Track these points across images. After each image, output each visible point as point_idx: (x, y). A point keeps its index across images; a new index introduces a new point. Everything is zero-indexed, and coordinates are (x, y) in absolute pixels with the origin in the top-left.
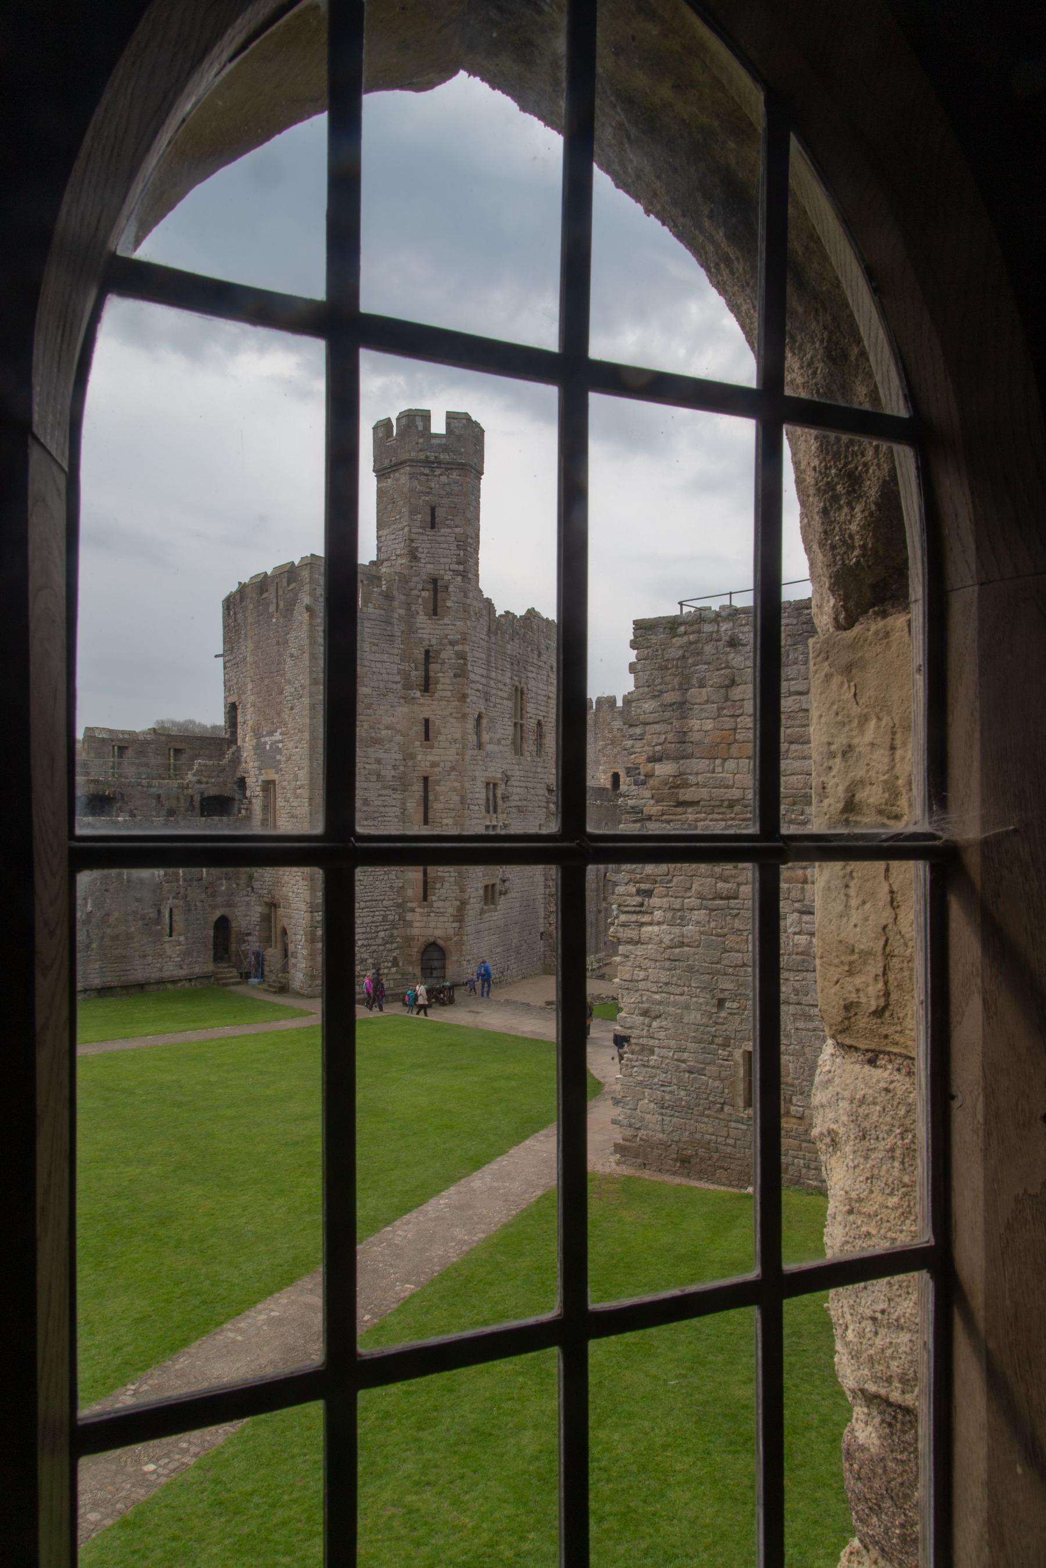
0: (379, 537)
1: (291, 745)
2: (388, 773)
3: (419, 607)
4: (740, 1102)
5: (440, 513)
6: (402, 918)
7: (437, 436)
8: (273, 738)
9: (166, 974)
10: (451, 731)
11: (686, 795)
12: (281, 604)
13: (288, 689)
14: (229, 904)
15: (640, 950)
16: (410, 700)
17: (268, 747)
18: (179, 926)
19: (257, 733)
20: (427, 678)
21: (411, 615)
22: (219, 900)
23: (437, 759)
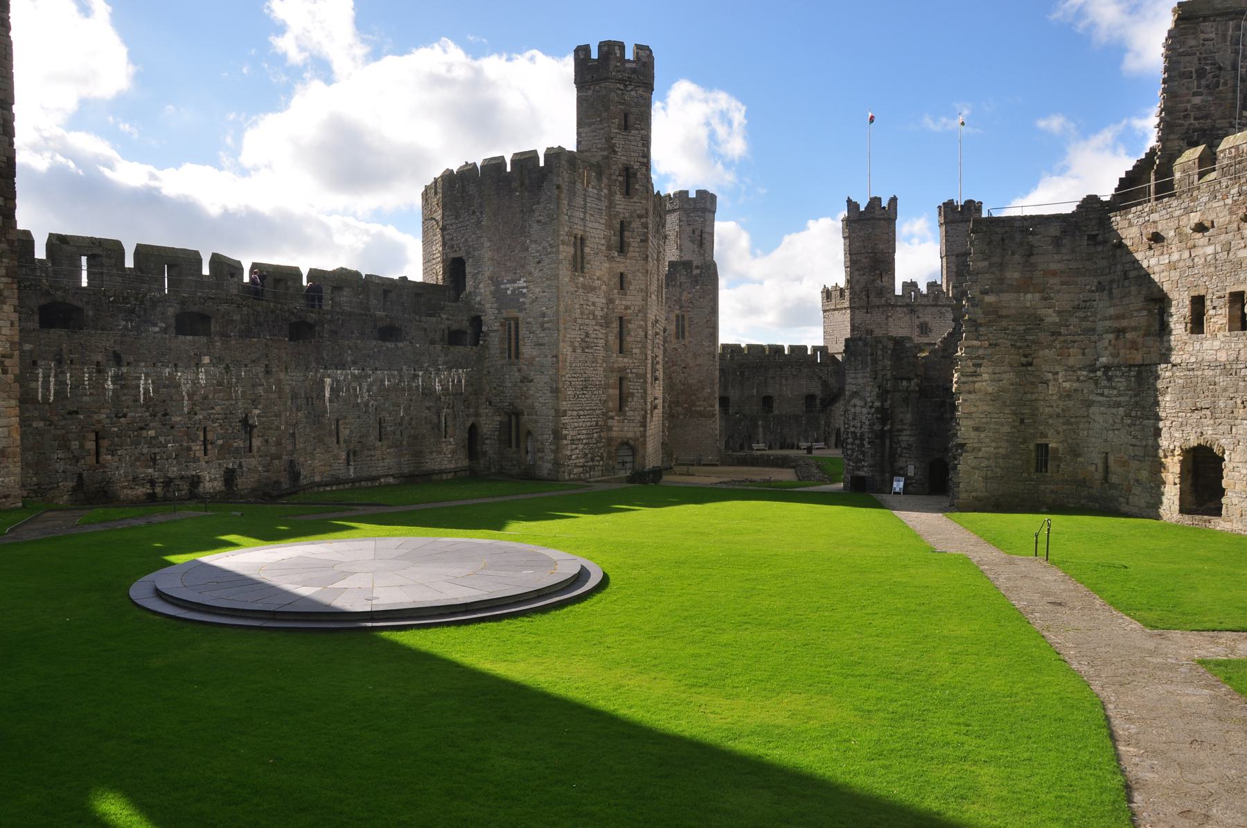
0: (578, 134)
1: (537, 290)
2: (598, 313)
4: (1032, 470)
6: (606, 423)
7: (629, 61)
9: (443, 467)
10: (636, 284)
11: (1004, 312)
12: (527, 182)
14: (477, 415)
15: (972, 396)
16: (611, 259)
18: (450, 430)
19: (495, 281)
21: (611, 194)
22: (471, 410)
23: (629, 303)
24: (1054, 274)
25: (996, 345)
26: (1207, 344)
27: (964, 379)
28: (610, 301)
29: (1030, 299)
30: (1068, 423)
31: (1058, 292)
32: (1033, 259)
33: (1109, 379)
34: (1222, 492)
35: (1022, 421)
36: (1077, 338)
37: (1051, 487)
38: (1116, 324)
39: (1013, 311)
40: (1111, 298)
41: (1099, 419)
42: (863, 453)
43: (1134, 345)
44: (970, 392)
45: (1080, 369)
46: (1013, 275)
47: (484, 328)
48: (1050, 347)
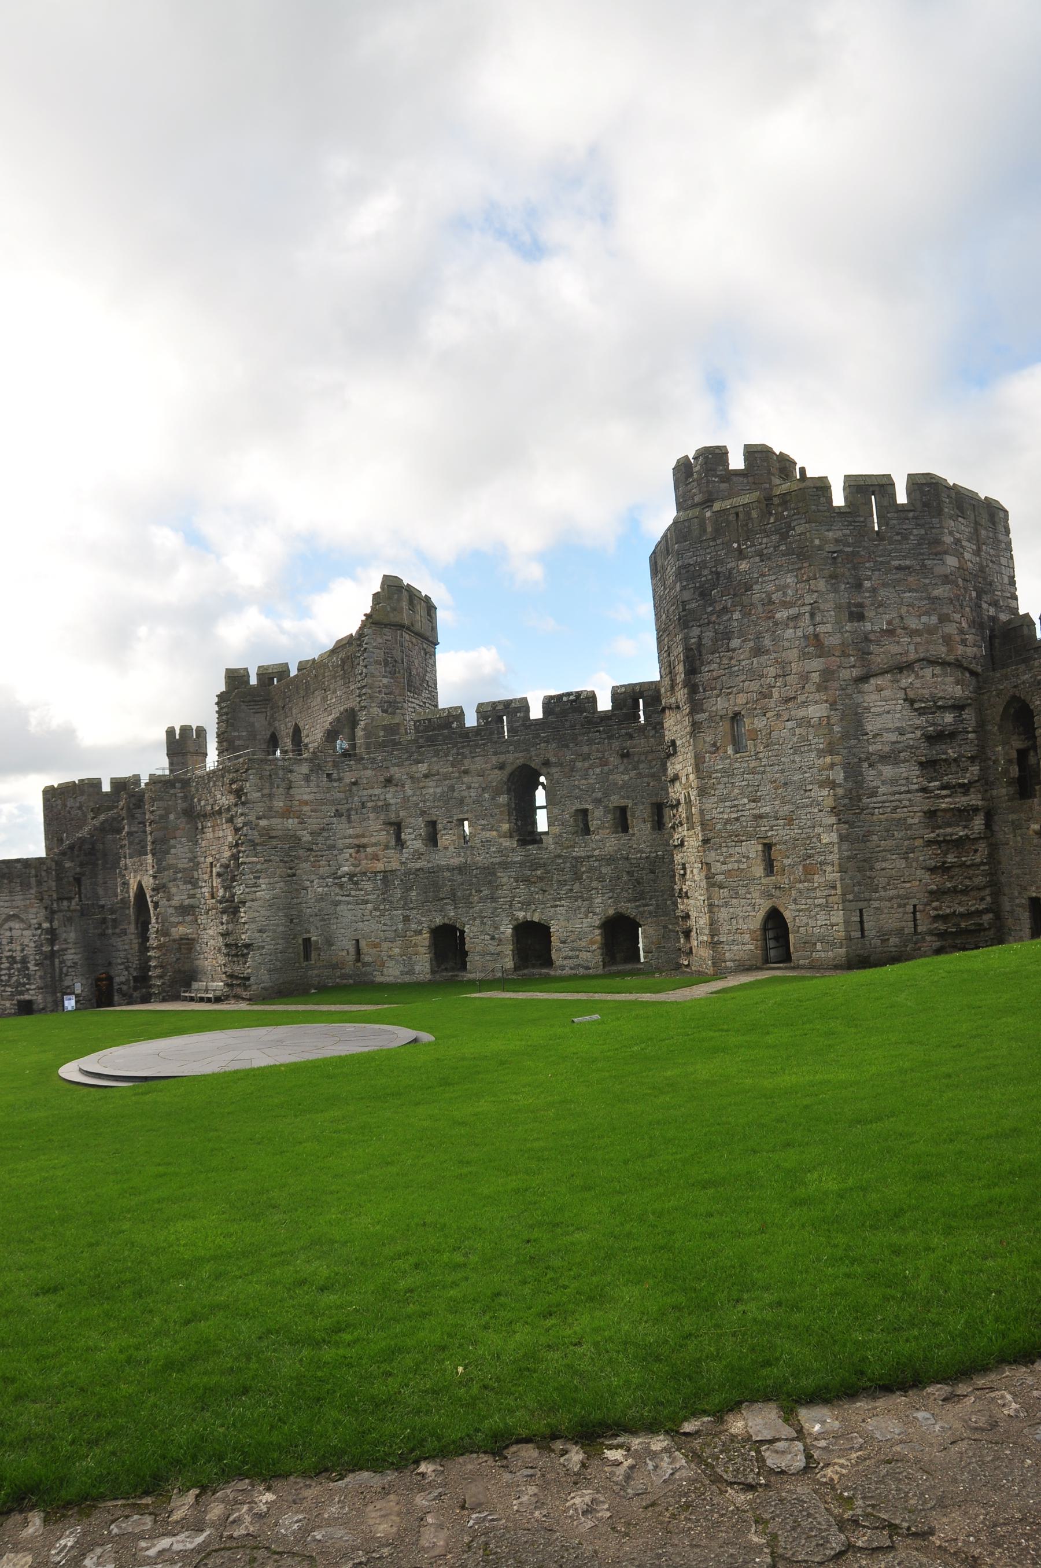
11: (273, 833)
15: (255, 904)
24: (306, 803)
25: (270, 861)
26: (441, 854)
27: (247, 890)
29: (291, 823)
30: (323, 920)
31: (310, 817)
32: (292, 791)
33: (356, 883)
34: (465, 954)
35: (291, 921)
36: (324, 853)
37: (316, 972)
38: (356, 841)
39: (280, 833)
40: (349, 822)
41: (349, 914)
42: (28, 977)
43: (376, 857)
44: (253, 900)
45: (328, 877)
48: (306, 861)
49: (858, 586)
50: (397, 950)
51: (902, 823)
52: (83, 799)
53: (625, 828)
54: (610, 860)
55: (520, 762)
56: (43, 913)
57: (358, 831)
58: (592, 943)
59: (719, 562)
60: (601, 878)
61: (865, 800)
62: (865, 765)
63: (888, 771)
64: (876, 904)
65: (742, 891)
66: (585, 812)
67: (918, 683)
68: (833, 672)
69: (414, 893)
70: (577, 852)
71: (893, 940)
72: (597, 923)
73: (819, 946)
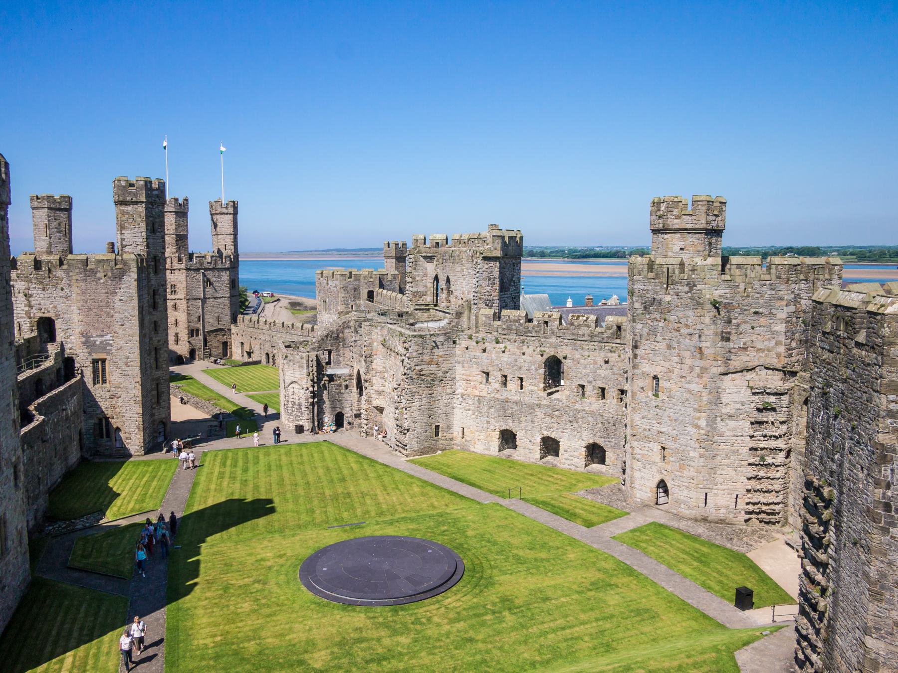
3: (151, 270)
5: (156, 226)
8: (104, 339)
13: (117, 316)
16: (150, 313)
17: (98, 343)
20: (154, 302)
21: (149, 274)
28: (151, 339)
29: (433, 367)
46: (426, 358)
47: (77, 365)
49: (729, 322)
50: (482, 437)
51: (736, 452)
52: (337, 282)
53: (603, 397)
54: (593, 414)
55: (552, 354)
56: (310, 383)
57: (467, 372)
58: (580, 454)
59: (656, 292)
60: (588, 423)
61: (716, 438)
62: (719, 419)
63: (731, 424)
64: (715, 491)
65: (648, 467)
66: (583, 387)
67: (757, 378)
68: (707, 369)
69: (492, 410)
70: (578, 406)
71: (723, 511)
72: (584, 445)
73: (682, 506)
